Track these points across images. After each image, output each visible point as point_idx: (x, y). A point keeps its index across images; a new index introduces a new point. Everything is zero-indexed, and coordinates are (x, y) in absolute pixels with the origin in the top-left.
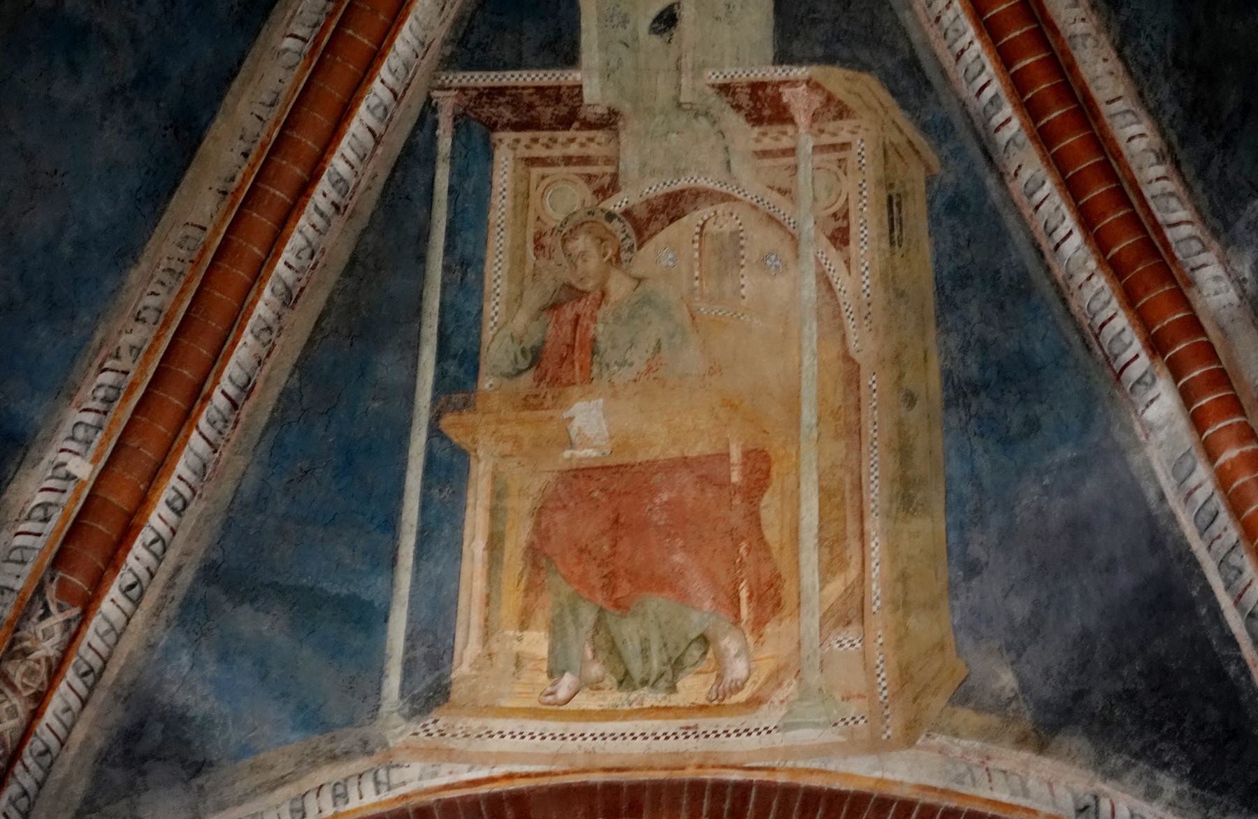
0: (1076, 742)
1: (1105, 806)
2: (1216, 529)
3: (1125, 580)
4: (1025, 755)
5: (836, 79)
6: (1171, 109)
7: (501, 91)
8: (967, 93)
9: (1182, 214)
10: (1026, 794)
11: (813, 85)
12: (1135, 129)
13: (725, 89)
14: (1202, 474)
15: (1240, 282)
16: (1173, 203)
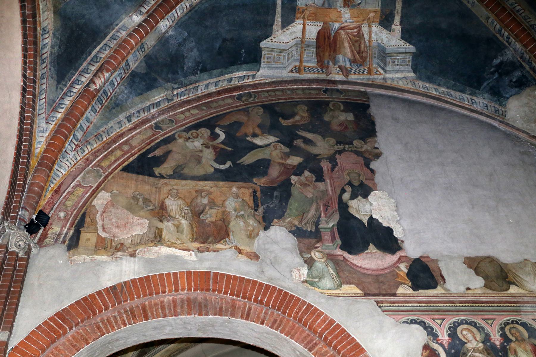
0: (59, 23)
1: (47, 36)
2: (113, 40)
3: (97, 22)
4: (52, 9)
6: (203, 7)
9: (179, 14)
10: (43, 13)
14: (124, 34)
15: (167, 32)
16: (181, 11)
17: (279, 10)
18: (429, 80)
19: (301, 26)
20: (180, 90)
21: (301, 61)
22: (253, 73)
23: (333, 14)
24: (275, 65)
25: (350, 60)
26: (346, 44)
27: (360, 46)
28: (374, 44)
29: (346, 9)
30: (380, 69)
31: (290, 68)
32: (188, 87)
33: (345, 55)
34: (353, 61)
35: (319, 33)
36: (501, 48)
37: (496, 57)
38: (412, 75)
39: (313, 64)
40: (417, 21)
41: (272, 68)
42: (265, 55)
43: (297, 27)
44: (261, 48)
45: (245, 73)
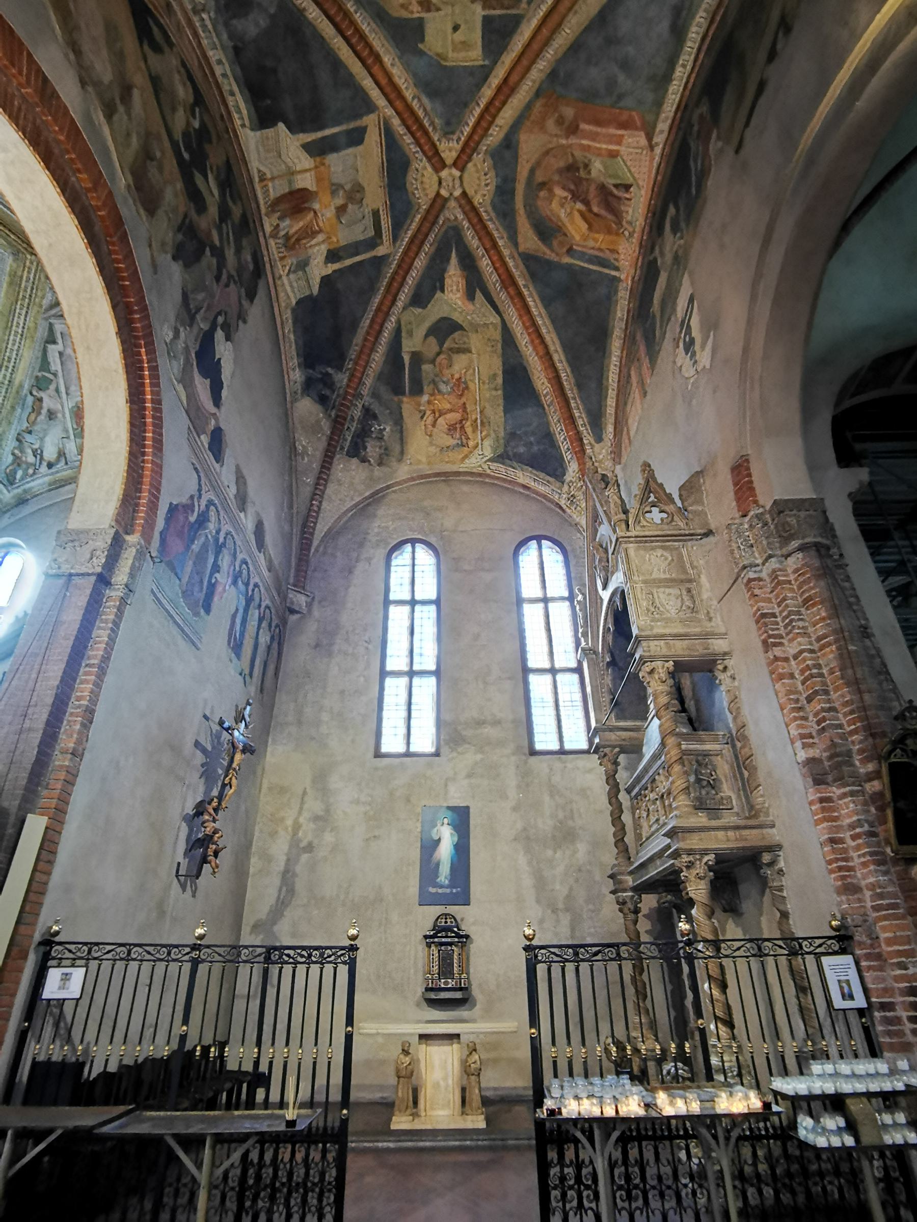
5: (405, 14)
7: (507, 8)
8: (365, 14)
11: (412, 12)
12: (314, 14)
13: (438, 9)
17: (319, 134)
18: (295, 322)
19: (307, 167)
20: (208, 23)
21: (273, 179)
22: (247, 123)
23: (325, 197)
24: (261, 149)
25: (287, 233)
26: (301, 224)
27: (304, 238)
28: (310, 251)
29: (334, 211)
30: (288, 268)
31: (262, 168)
32: (214, 35)
33: (291, 226)
34: (287, 237)
35: (305, 190)
36: (340, 368)
37: (332, 367)
38: (294, 302)
39: (273, 195)
40: (340, 286)
41: (257, 148)
42: (270, 132)
43: (305, 162)
44: (276, 124)
45: (245, 112)
